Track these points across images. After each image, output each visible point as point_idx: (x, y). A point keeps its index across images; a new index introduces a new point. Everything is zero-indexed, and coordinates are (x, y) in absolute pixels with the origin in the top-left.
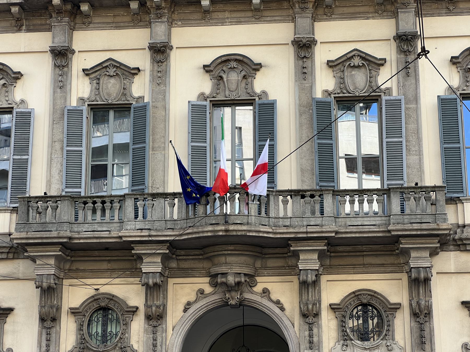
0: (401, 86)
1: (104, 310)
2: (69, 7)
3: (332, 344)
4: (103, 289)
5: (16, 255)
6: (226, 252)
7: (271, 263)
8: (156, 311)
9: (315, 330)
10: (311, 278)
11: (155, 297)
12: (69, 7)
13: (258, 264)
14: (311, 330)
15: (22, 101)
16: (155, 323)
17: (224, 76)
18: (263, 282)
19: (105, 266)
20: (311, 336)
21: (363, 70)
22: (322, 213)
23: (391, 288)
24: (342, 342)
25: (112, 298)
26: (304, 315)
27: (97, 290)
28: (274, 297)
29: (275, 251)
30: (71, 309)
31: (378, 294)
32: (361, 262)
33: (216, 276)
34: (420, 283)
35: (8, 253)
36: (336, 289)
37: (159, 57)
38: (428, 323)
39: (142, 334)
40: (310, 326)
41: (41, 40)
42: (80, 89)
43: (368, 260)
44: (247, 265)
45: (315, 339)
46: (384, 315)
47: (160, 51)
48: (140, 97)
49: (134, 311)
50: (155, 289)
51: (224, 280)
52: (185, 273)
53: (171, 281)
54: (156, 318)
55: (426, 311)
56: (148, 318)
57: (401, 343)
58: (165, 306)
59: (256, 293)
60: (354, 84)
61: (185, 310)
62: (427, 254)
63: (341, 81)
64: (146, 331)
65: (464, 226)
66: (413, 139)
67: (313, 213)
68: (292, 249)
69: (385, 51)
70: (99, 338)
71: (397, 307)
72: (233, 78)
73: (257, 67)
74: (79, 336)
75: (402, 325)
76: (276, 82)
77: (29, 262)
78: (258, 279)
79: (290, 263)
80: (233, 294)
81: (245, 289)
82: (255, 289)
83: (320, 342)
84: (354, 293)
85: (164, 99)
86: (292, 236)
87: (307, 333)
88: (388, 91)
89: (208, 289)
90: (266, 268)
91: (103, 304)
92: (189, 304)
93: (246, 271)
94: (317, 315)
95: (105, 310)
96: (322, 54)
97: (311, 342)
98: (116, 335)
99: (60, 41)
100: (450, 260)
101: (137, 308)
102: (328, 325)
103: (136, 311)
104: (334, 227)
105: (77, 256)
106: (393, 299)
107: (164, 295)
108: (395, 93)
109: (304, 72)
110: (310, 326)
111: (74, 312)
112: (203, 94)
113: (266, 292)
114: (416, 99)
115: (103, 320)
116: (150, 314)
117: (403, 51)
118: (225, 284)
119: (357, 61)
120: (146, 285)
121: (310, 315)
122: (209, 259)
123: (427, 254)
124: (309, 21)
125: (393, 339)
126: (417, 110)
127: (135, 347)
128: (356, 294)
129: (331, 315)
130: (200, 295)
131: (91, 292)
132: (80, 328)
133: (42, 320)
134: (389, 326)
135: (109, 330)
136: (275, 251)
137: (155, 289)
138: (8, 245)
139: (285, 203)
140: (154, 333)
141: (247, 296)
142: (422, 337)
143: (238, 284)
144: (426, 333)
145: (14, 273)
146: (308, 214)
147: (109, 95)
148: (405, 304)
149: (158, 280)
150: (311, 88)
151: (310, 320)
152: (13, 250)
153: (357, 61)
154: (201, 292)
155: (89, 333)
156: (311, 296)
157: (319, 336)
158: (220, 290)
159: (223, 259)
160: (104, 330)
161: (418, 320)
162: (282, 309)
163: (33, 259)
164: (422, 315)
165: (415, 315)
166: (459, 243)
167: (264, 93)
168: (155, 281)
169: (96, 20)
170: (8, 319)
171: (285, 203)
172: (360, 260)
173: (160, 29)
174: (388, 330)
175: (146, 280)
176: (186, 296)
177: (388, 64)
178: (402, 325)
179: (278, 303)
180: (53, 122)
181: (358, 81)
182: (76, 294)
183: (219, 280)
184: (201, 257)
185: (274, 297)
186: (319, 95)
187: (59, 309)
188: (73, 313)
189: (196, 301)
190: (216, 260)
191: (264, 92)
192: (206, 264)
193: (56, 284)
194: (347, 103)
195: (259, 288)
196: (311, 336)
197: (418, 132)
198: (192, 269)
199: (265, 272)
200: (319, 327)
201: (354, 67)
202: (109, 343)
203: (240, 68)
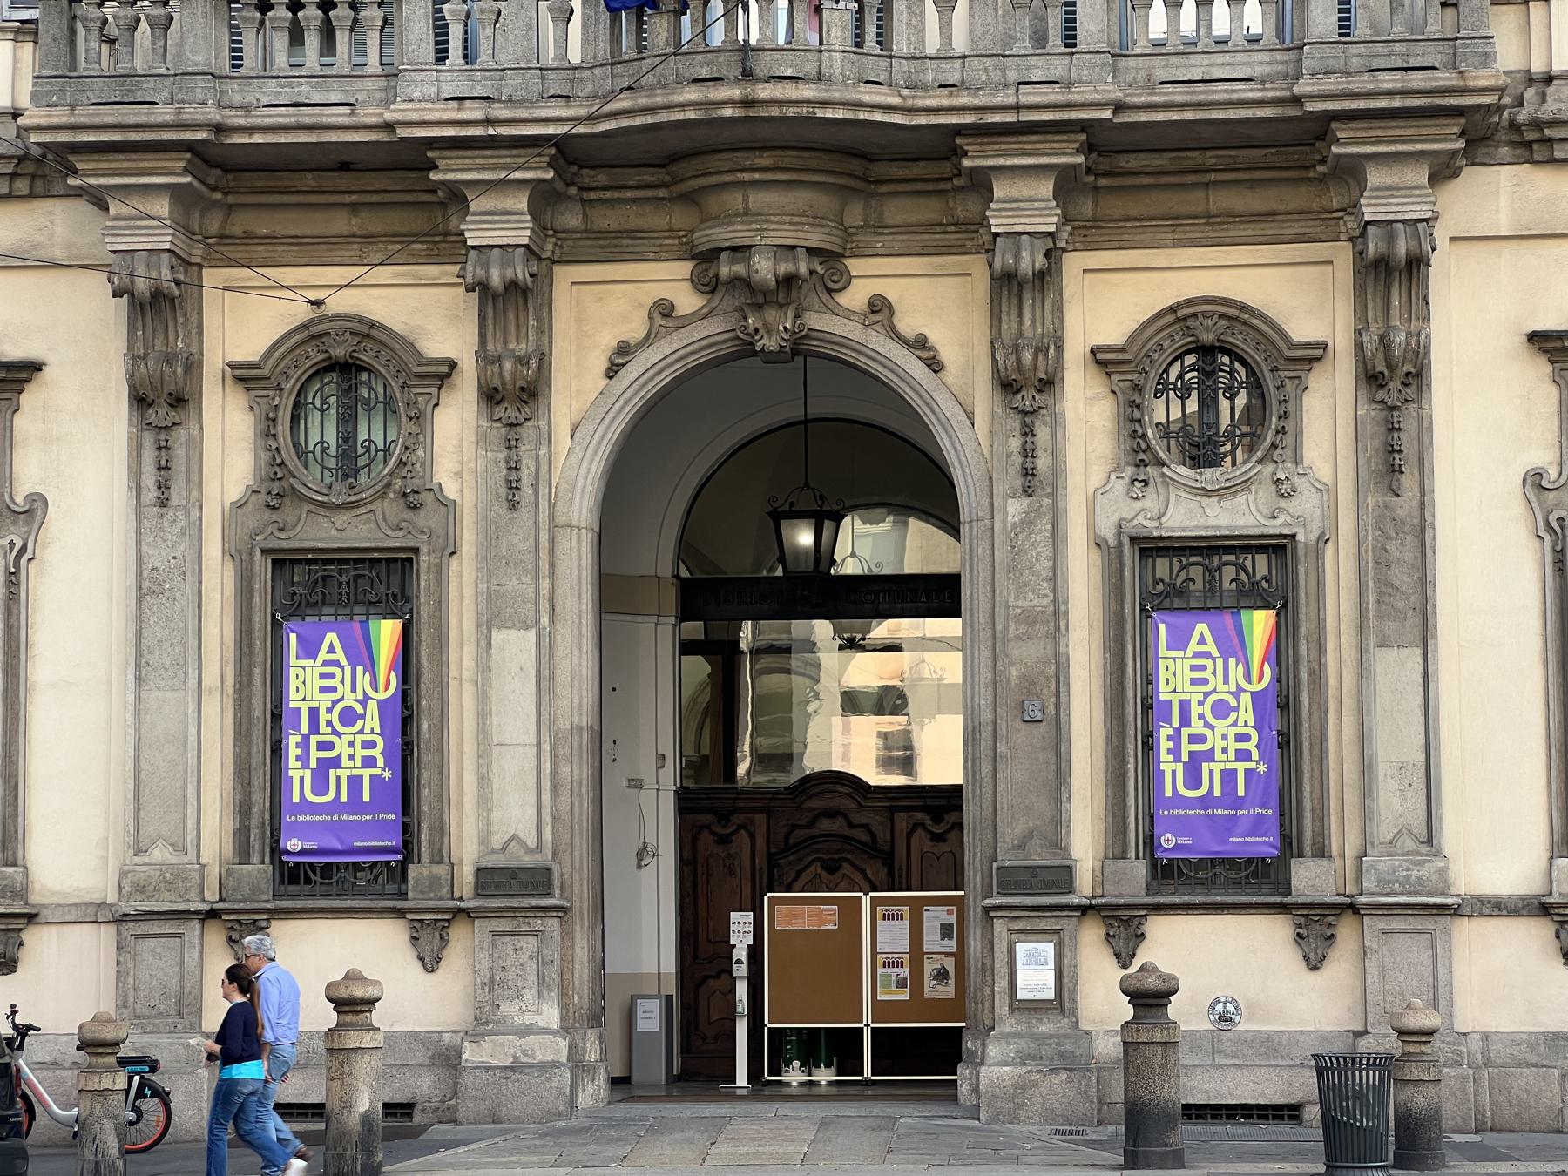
1: (340, 368)
3: (1096, 479)
4: (339, 303)
5: (39, 183)
6: (746, 176)
7: (898, 211)
8: (514, 373)
9: (1043, 434)
10: (1030, 261)
11: (512, 329)
13: (855, 215)
14: (1028, 432)
16: (513, 414)
18: (869, 277)
19: (341, 223)
20: (1028, 453)
22: (1070, 39)
23: (1295, 291)
24: (1129, 471)
25: (367, 330)
26: (1007, 386)
27: (317, 303)
28: (907, 324)
29: (912, 172)
30: (232, 366)
31: (1253, 312)
32: (1200, 209)
33: (713, 255)
34: (1393, 272)
35: (13, 176)
36: (1112, 298)
38: (1412, 407)
39: (469, 449)
44: (818, 220)
45: (1043, 463)
46: (1270, 382)
50: (509, 302)
51: (739, 269)
52: (610, 247)
53: (564, 275)
54: (514, 396)
55: (1408, 368)
56: (491, 396)
57: (1323, 472)
58: (544, 358)
59: (848, 314)
61: (612, 371)
62: (1420, 175)
64: (483, 439)
67: (1040, 39)
68: (966, 163)
70: (332, 463)
71: (1313, 355)
74: (265, 456)
75: (1328, 415)
77: (82, 210)
78: (855, 265)
79: (960, 213)
80: (771, 314)
81: (811, 299)
82: (844, 299)
83: (1057, 471)
84: (1171, 310)
86: (969, 119)
87: (1015, 443)
89: (687, 301)
90: (877, 228)
91: (339, 352)
93: (814, 238)
94: (1049, 384)
95: (348, 369)
97: (1028, 473)
98: (387, 452)
101: (453, 365)
102: (1086, 415)
103: (449, 375)
104: (1110, 90)
105: (245, 188)
106: (1301, 329)
107: (540, 320)
111: (244, 376)
113: (879, 308)
115: (341, 406)
116: (496, 382)
118: (743, 283)
120: (481, 288)
121: (1026, 385)
122: (690, 199)
123: (1420, 175)
125: (1297, 461)
127: (451, 491)
128: (1179, 315)
130: (659, 321)
131: (295, 311)
132: (267, 431)
133: (140, 400)
134: (1284, 416)
135: (362, 435)
137: (509, 302)
138: (12, 151)
140: (511, 445)
141: (817, 321)
142: (1392, 450)
143: (789, 282)
144: (1406, 440)
145: (36, 246)
146: (1024, 45)
149: (520, 272)
151: (1027, 400)
152: (29, 168)
154: (664, 310)
155: (296, 445)
156: (1031, 322)
157: (1056, 453)
158: (725, 301)
159: (735, 200)
161: (1381, 394)
162: (935, 365)
163: (98, 200)
164: (1394, 380)
165: (1371, 379)
166: (1530, 135)
168: (509, 274)
170: (24, 398)
172: (1195, 201)
174: (1282, 431)
175: (480, 273)
176: (615, 323)
178: (1328, 415)
179: (919, 344)
182: (247, 318)
183: (725, 270)
184: (661, 193)
185: (907, 324)
187: (193, 366)
188: (240, 379)
189: (646, 341)
190: (713, 203)
192: (679, 217)
193: (178, 283)
195: (855, 297)
196: (1028, 453)
198: (633, 233)
199: (879, 242)
200: (1056, 423)
202: (362, 477)
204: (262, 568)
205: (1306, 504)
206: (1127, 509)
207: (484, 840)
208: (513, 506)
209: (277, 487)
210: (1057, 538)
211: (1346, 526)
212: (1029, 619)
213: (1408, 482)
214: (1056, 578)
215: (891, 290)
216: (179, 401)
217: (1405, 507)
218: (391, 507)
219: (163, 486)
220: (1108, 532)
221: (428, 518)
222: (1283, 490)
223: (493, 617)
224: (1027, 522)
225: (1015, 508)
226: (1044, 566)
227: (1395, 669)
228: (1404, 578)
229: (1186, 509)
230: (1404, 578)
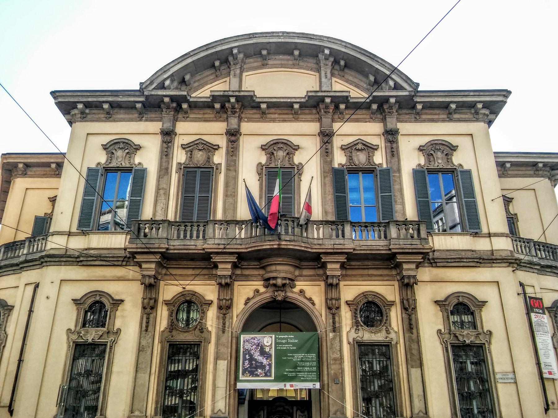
1: (188, 302)
2: (174, 105)
3: (348, 329)
4: (188, 288)
5: (128, 263)
7: (306, 272)
8: (225, 303)
9: (337, 319)
10: (335, 281)
11: (225, 294)
12: (174, 105)
13: (297, 273)
14: (334, 318)
15: (140, 164)
16: (225, 312)
17: (275, 152)
18: (300, 285)
20: (334, 323)
21: (364, 152)
23: (387, 290)
24: (355, 327)
25: (194, 294)
27: (184, 288)
30: (164, 301)
31: (380, 294)
33: (268, 279)
35: (123, 261)
36: (350, 291)
37: (233, 138)
38: (414, 315)
39: (215, 320)
41: (156, 126)
42: (179, 156)
43: (371, 272)
44: (291, 273)
45: (337, 325)
46: (383, 309)
47: (233, 135)
48: (219, 164)
49: (210, 303)
51: (274, 282)
52: (247, 278)
53: (236, 283)
54: (225, 308)
55: (413, 307)
56: (220, 308)
57: (396, 329)
58: (231, 299)
59: (295, 293)
60: (359, 160)
61: (246, 304)
63: (350, 158)
64: (218, 318)
65: (434, 251)
66: (398, 194)
70: (184, 323)
74: (170, 321)
75: (395, 316)
77: (137, 268)
78: (297, 283)
80: (280, 292)
81: (288, 289)
82: (294, 290)
83: (340, 327)
84: (363, 293)
85: (235, 165)
87: (331, 321)
89: (262, 290)
91: (188, 298)
92: (248, 299)
93: (290, 276)
94: (338, 308)
95: (189, 303)
96: (338, 142)
98: (196, 320)
99: (168, 125)
100: (426, 273)
101: (212, 302)
102: (346, 316)
103: (211, 304)
106: (390, 298)
107: (231, 292)
108: (385, 166)
109: (326, 151)
111: (167, 303)
112: (260, 163)
113: (302, 291)
114: (399, 170)
115: (187, 310)
116: (221, 305)
117: (388, 141)
118: (275, 285)
120: (220, 284)
121: (333, 308)
122: (263, 268)
124: (330, 120)
125: (390, 326)
126: (400, 177)
127: (210, 329)
128: (364, 294)
129: (347, 308)
130: (256, 293)
131: (179, 289)
132: (170, 315)
133: (144, 308)
134: (387, 317)
135: (191, 316)
136: (311, 261)
138: (122, 255)
139: (318, 229)
141: (289, 294)
142: (410, 324)
143: (284, 285)
144: (413, 322)
145: (126, 276)
147: (198, 161)
148: (398, 301)
150: (331, 161)
152: (126, 259)
153: (360, 146)
154: (257, 291)
155: (177, 318)
156: (334, 295)
157: (340, 323)
158: (270, 289)
159: (273, 268)
160: (188, 317)
161: (407, 312)
162: (313, 304)
164: (409, 309)
165: (405, 309)
166: (432, 261)
169: (192, 116)
170: (119, 308)
171: (318, 229)
173: (234, 121)
174: (387, 320)
177: (379, 150)
178: (395, 316)
179: (310, 299)
181: (361, 158)
182: (170, 290)
183: (272, 282)
184: (258, 267)
186: (336, 166)
187: (156, 301)
188: (166, 304)
189: (253, 298)
190: (269, 269)
192: (261, 272)
193: (155, 282)
194: (354, 171)
196: (334, 323)
197: (401, 190)
198: (251, 276)
199: (302, 278)
200: (340, 317)
201: (358, 150)
202: (190, 326)
203: (285, 148)
204: (167, 345)
205: (393, 335)
206: (355, 336)
207: (213, 410)
208: (224, 332)
209: (172, 326)
210: (341, 342)
211: (402, 341)
212: (335, 359)
213: (414, 331)
214: (341, 350)
215: (304, 288)
216: (152, 308)
217: (414, 336)
218: (197, 332)
219: (147, 327)
220: (351, 341)
221: (204, 335)
222: (388, 332)
223: (217, 358)
224: (334, 338)
225: (331, 335)
226: (338, 348)
227: (415, 372)
228: (415, 352)
229: (368, 336)
230: (415, 352)
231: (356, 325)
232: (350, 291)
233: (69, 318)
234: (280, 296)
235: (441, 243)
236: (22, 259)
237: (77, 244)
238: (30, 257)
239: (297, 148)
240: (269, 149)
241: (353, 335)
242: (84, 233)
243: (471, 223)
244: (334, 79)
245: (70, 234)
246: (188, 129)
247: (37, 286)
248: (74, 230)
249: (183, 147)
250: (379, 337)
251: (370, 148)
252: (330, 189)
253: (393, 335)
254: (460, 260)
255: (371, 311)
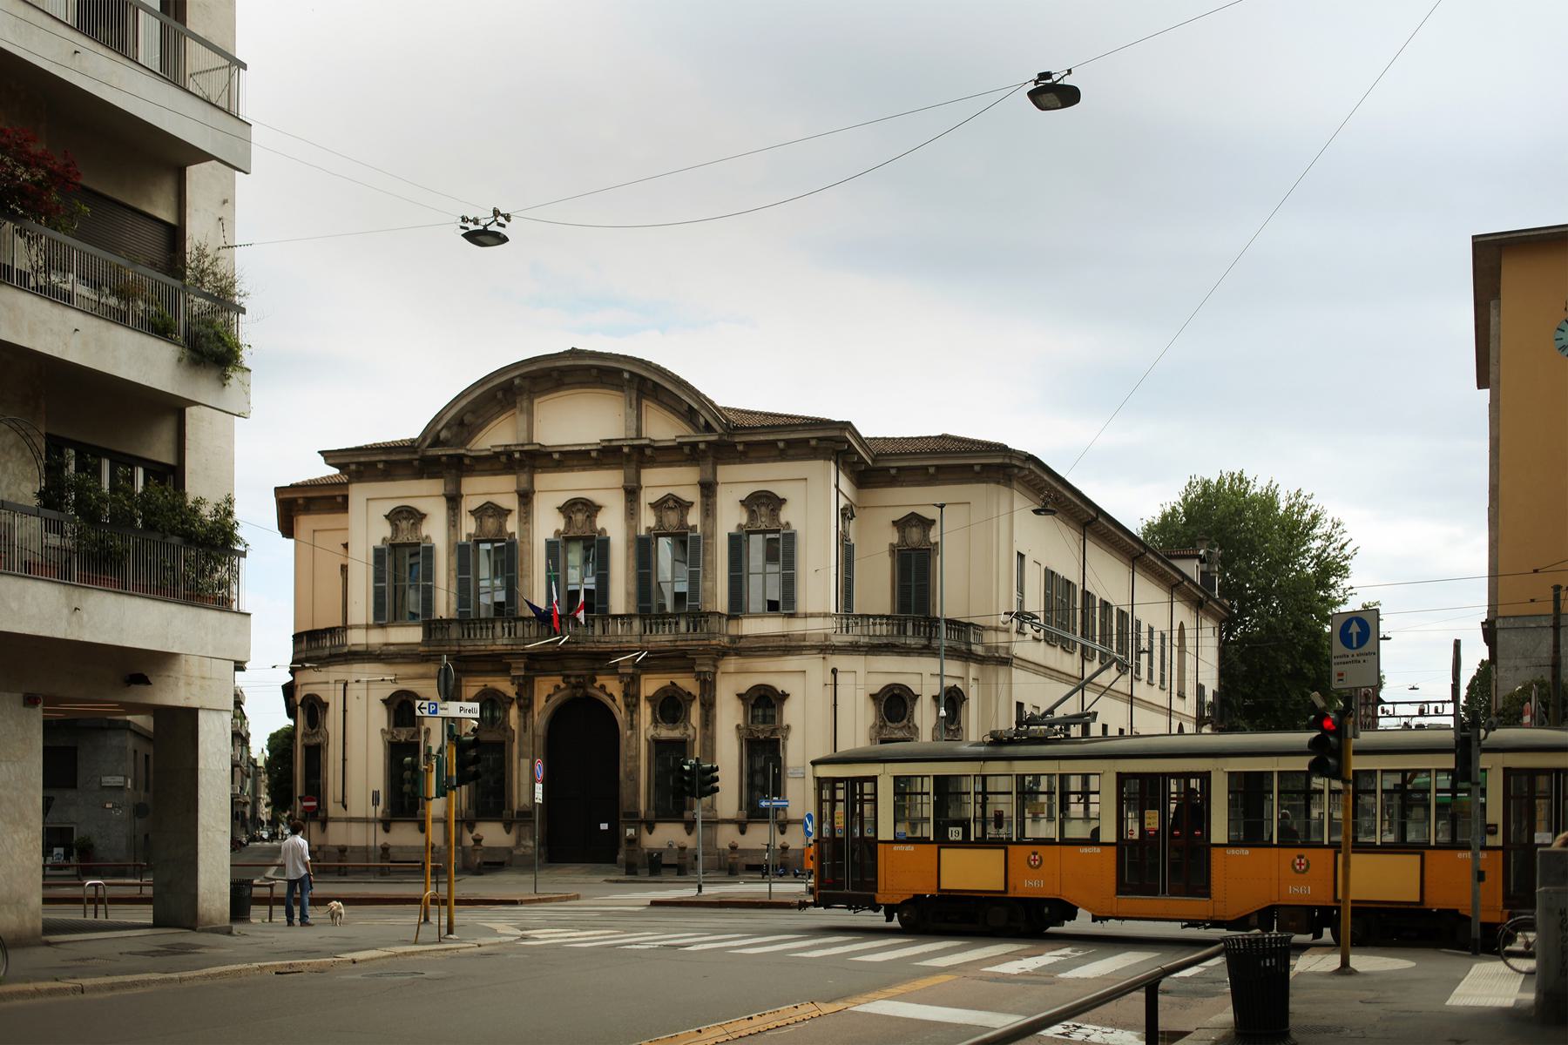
0: (703, 525)
26: (627, 706)
28: (609, 690)
40: (632, 713)
42: (469, 526)
52: (546, 673)
69: (691, 494)
72: (579, 517)
73: (598, 508)
75: (695, 712)
76: (612, 523)
88: (694, 528)
94: (637, 705)
102: (645, 712)
109: (632, 512)
110: (632, 713)
113: (603, 687)
114: (713, 535)
119: (671, 504)
121: (632, 707)
128: (663, 690)
154: (558, 687)
162: (614, 700)
167: (603, 530)
176: (546, 690)
179: (611, 696)
180: (449, 555)
191: (603, 530)
195: (597, 685)
197: (713, 563)
205: (691, 732)
222: (686, 728)
229: (665, 733)
231: (655, 722)
232: (651, 685)
233: (380, 718)
234: (579, 693)
235: (751, 627)
236: (327, 652)
237: (376, 638)
238: (334, 651)
239: (598, 508)
240: (568, 509)
241: (651, 732)
242: (382, 626)
243: (782, 606)
244: (645, 402)
245: (368, 627)
246: (479, 489)
247: (346, 684)
248: (371, 621)
249: (472, 513)
250: (676, 734)
251: (683, 506)
252: (633, 563)
253: (691, 732)
254: (765, 649)
255: (670, 707)
